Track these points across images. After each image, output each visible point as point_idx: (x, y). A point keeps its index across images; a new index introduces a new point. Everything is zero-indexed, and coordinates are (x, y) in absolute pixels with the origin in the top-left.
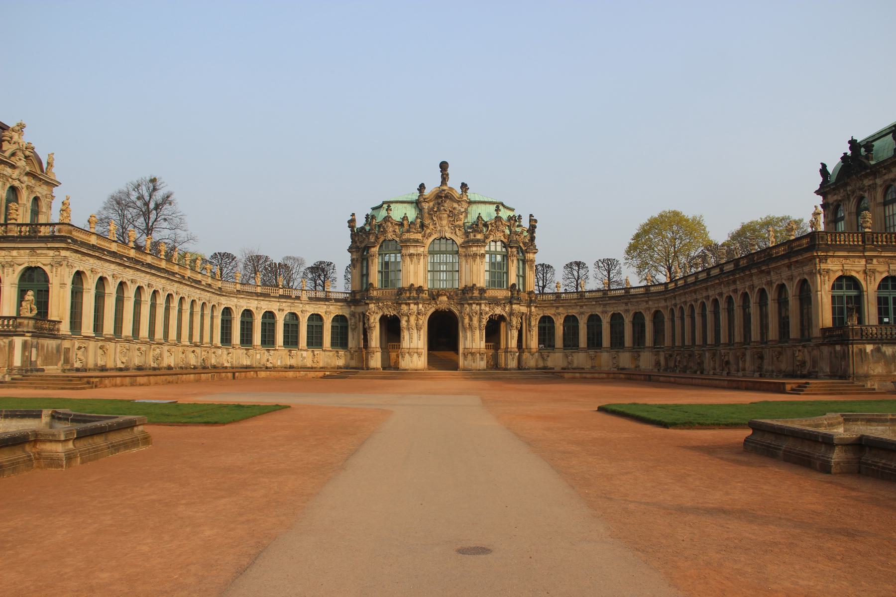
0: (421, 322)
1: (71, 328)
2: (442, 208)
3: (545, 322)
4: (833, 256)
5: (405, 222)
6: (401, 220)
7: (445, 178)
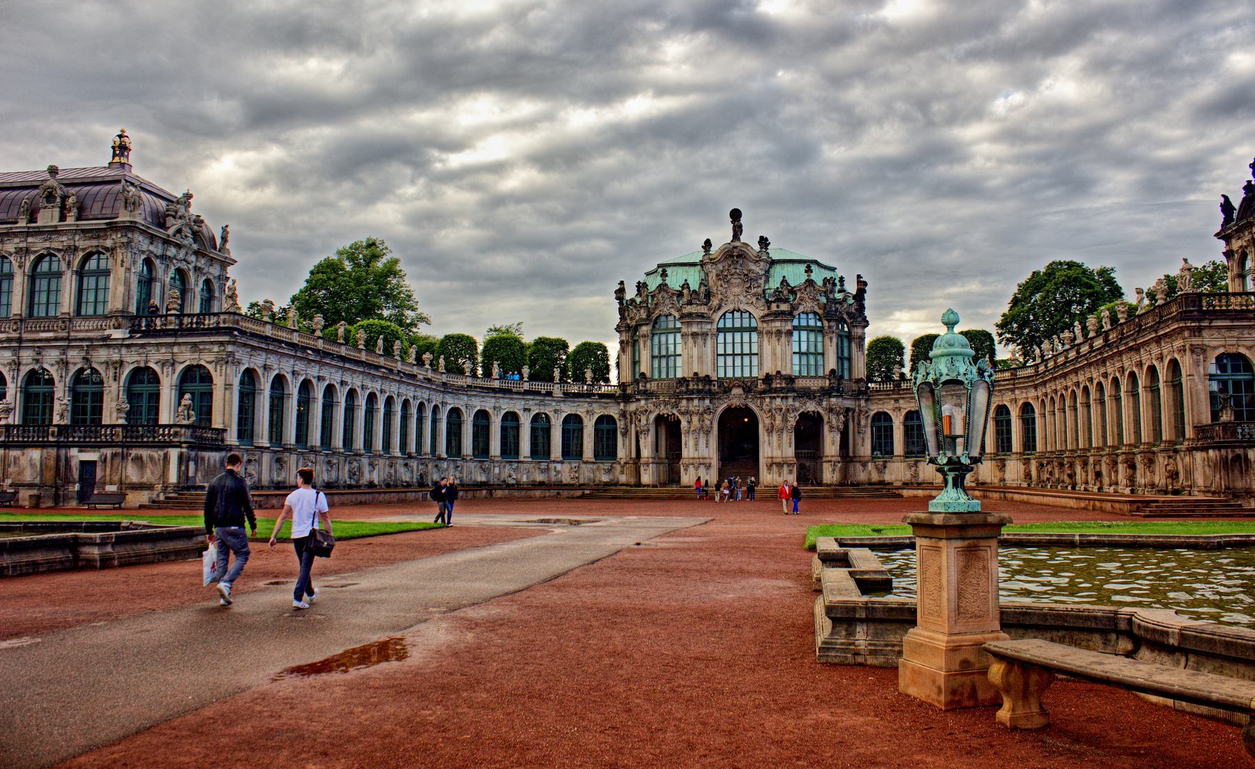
0: (708, 423)
1: (238, 438)
2: (733, 271)
3: (879, 420)
4: (1210, 327)
5: (685, 291)
6: (680, 289)
7: (737, 231)
